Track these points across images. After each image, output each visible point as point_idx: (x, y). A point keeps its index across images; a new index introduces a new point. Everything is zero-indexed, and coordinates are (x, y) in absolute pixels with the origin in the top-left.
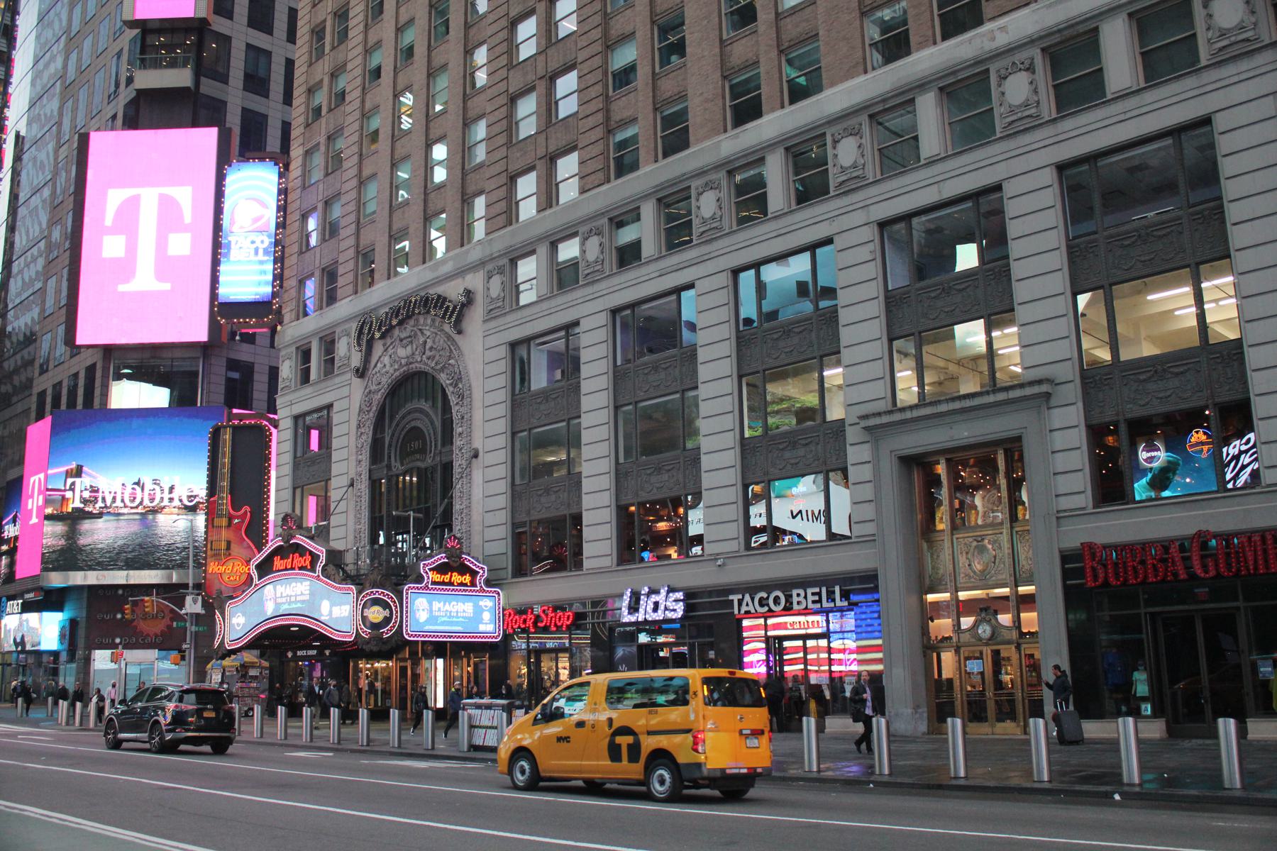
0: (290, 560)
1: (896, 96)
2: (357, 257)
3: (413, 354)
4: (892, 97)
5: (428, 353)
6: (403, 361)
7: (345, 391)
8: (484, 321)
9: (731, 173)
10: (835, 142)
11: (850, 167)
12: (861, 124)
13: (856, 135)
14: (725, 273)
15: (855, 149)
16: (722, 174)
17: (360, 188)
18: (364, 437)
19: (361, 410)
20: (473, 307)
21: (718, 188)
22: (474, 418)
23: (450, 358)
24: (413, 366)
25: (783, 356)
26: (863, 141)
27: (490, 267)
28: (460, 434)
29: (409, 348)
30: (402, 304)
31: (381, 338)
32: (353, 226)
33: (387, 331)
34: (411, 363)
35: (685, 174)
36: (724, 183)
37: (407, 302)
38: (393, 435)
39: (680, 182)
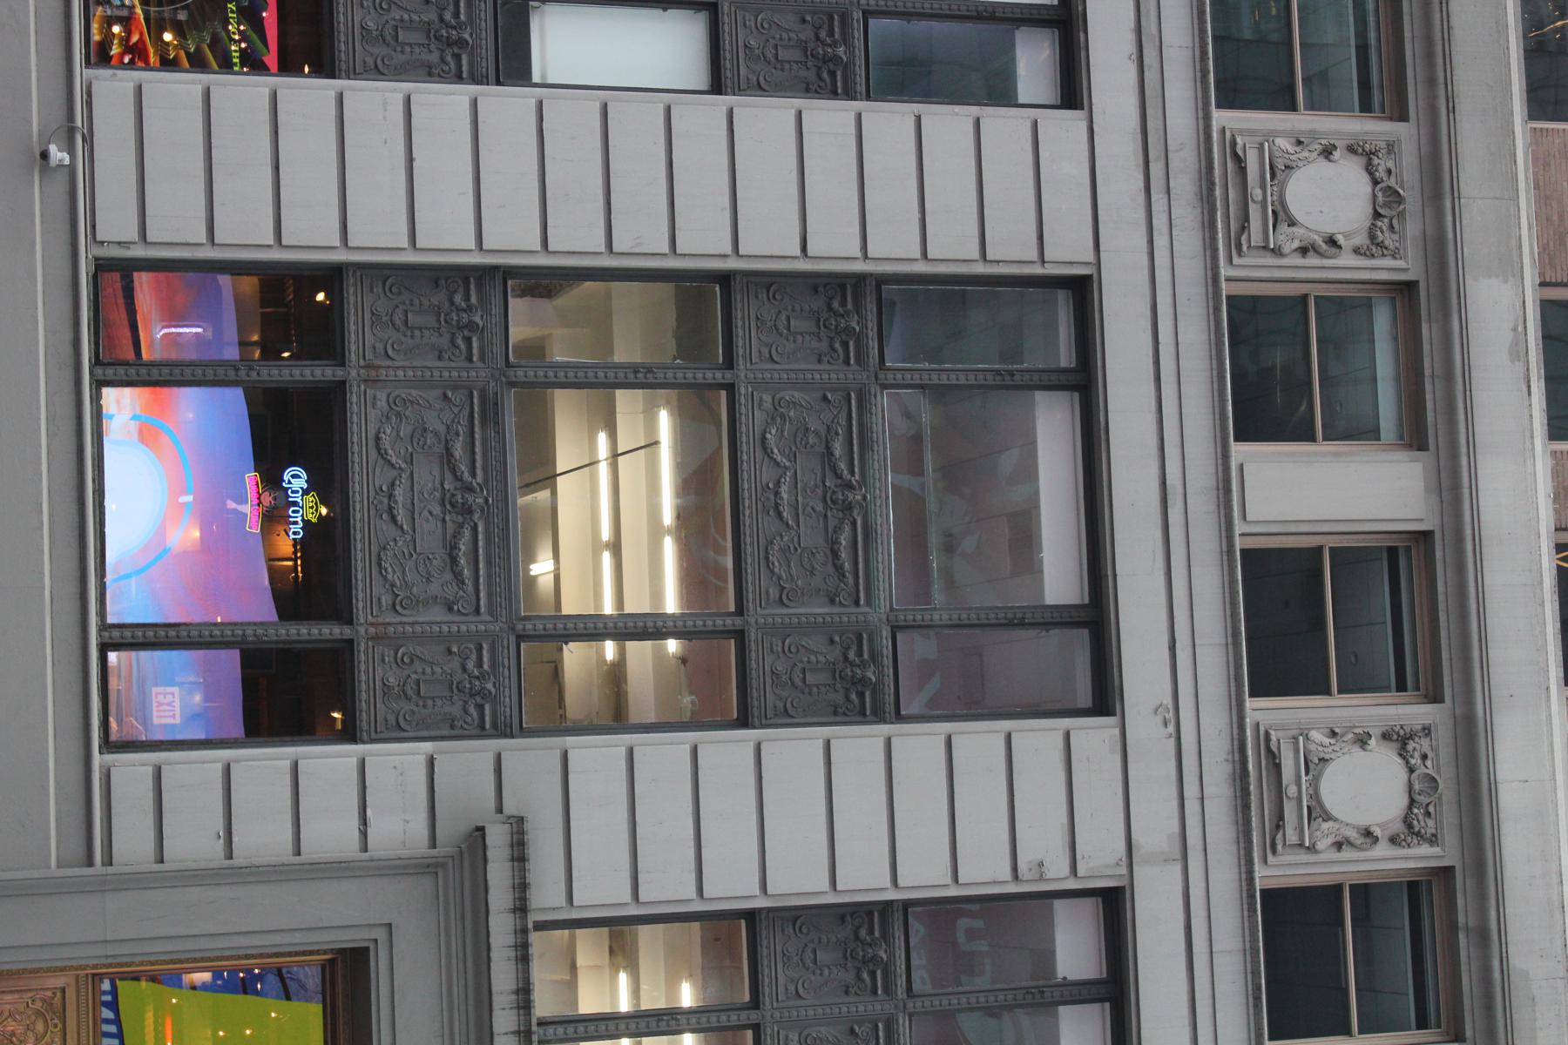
1: (1487, 981)
4: (1486, 969)
9: (1404, 291)
10: (1400, 740)
11: (1315, 796)
12: (1433, 840)
13: (1407, 821)
14: (1089, 256)
15: (1363, 820)
16: (1407, 266)
21: (1374, 246)
25: (767, 474)
26: (1383, 849)
35: (1451, 110)
36: (1384, 268)
39: (1431, 82)
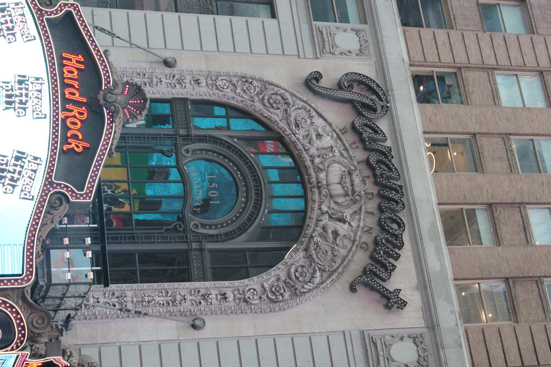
0: (77, 97)
2: (455, 67)
3: (331, 196)
5: (332, 225)
6: (322, 175)
7: (291, 49)
8: (362, 333)
17: (536, 71)
18: (229, 93)
19: (266, 84)
20: (382, 308)
22: (244, 316)
23: (322, 271)
24: (316, 197)
27: (428, 340)
28: (224, 297)
29: (337, 190)
30: (394, 175)
31: (353, 127)
32: (491, 62)
33: (362, 141)
34: (319, 188)
37: (399, 190)
38: (230, 146)
